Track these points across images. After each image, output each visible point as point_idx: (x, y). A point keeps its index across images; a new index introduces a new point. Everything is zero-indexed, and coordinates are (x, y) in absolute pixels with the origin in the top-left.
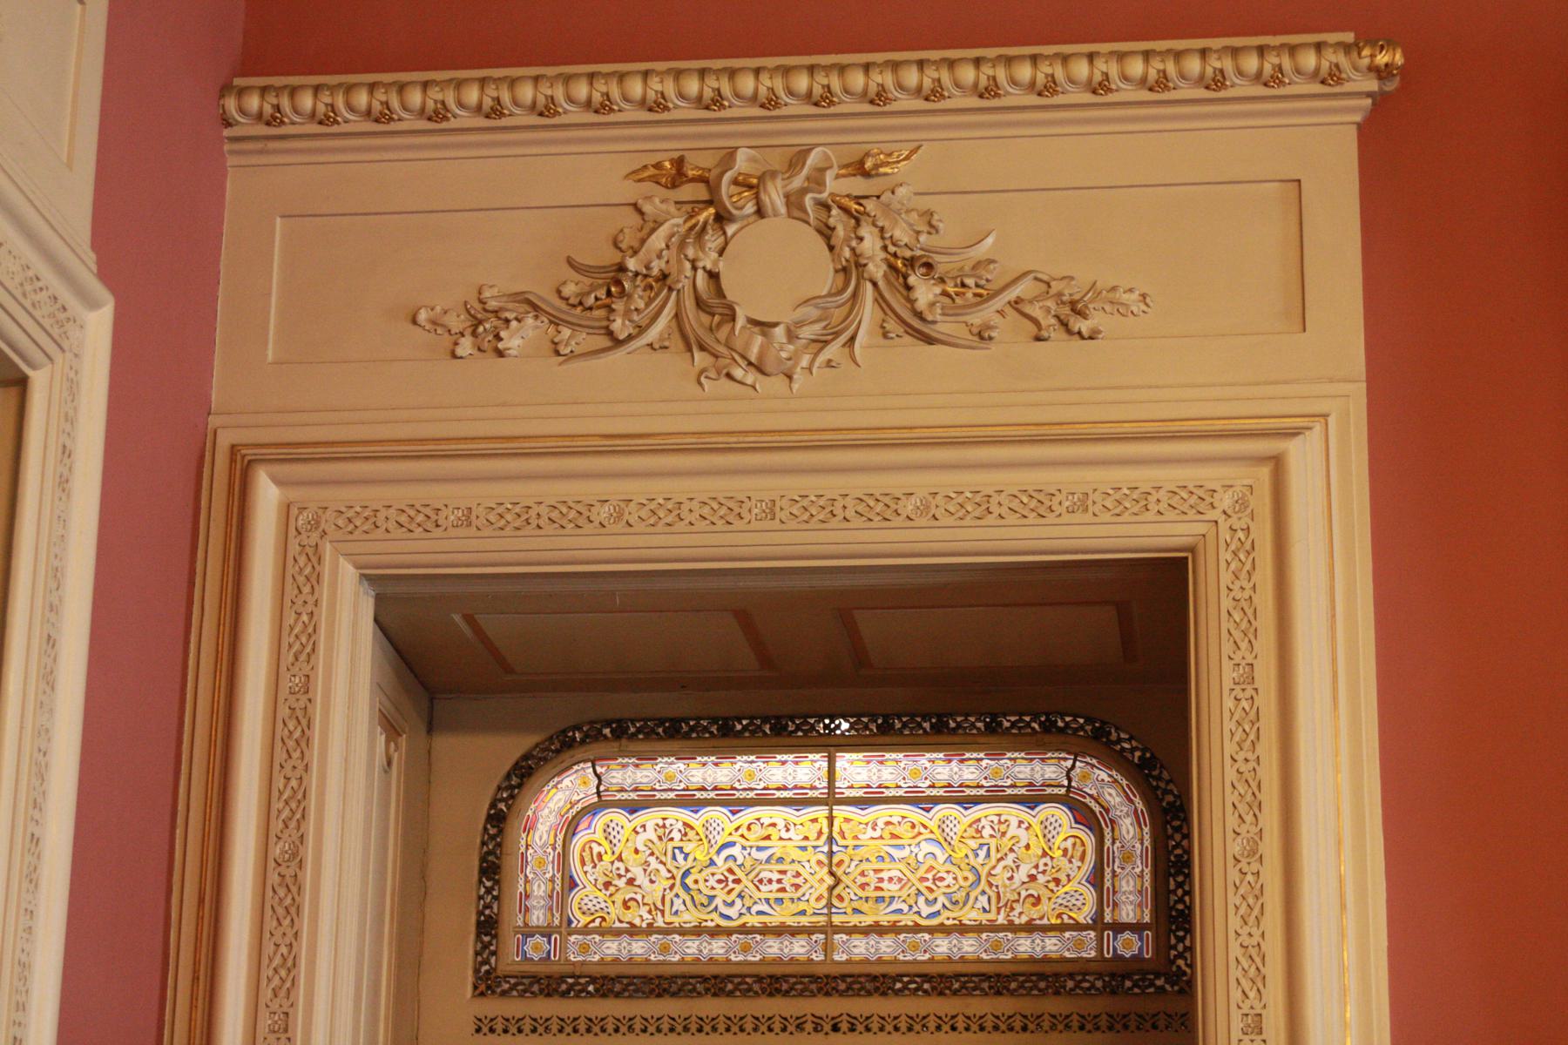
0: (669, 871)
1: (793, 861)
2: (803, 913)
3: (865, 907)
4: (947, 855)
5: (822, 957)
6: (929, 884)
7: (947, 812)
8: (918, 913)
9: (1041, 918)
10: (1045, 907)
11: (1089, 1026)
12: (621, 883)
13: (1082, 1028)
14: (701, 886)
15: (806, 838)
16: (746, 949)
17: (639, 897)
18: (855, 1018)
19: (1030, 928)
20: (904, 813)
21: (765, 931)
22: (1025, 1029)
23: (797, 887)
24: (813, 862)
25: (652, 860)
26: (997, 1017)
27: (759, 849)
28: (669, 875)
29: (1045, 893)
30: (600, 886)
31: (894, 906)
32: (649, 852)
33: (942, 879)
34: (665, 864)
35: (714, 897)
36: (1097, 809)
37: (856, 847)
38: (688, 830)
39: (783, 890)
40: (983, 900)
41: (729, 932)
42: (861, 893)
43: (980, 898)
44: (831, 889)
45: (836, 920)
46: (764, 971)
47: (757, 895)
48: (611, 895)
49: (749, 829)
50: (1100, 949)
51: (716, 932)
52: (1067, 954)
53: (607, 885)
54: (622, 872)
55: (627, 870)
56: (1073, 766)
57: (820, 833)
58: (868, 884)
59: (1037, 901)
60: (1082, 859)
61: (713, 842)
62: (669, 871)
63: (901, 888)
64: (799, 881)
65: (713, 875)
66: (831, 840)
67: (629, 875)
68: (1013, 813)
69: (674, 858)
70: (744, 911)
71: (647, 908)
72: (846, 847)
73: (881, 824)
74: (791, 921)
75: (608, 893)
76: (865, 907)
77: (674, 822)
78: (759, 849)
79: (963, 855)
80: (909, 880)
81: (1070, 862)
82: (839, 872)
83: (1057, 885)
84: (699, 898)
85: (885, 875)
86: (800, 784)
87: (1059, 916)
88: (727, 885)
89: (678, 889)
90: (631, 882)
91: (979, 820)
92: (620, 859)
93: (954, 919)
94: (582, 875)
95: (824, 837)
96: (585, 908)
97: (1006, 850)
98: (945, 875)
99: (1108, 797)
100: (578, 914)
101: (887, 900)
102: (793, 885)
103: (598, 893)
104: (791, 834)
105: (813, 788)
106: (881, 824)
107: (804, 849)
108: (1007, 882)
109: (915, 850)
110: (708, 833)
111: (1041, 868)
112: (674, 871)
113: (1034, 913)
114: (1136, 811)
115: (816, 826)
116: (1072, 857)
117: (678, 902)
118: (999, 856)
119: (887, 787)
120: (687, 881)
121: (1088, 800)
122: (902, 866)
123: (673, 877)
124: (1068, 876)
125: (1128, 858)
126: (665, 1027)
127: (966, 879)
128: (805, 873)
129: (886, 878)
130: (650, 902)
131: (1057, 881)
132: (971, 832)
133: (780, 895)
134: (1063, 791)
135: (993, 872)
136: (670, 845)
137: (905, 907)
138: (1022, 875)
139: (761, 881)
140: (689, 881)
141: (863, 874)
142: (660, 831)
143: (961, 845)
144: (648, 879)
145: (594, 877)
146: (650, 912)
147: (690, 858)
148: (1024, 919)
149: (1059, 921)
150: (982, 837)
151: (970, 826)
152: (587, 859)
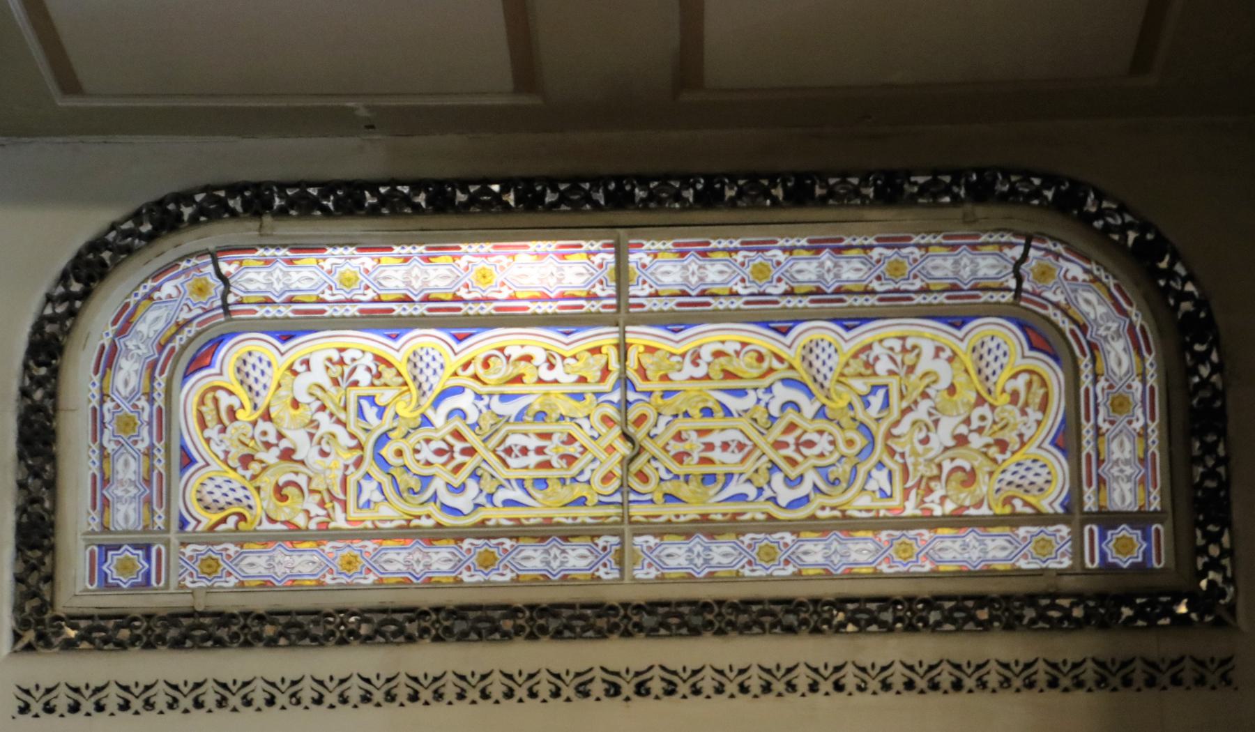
0: (353, 436)
1: (562, 417)
2: (581, 502)
3: (683, 491)
4: (817, 405)
5: (615, 574)
6: (790, 452)
7: (816, 335)
8: (773, 500)
9: (978, 505)
10: (984, 486)
11: (1065, 682)
12: (271, 456)
13: (1053, 683)
14: (408, 459)
15: (582, 380)
16: (487, 563)
17: (302, 480)
18: (674, 673)
19: (958, 521)
20: (745, 337)
21: (519, 532)
22: (957, 686)
23: (570, 459)
24: (596, 419)
25: (323, 417)
26: (911, 668)
27: (504, 397)
28: (353, 443)
29: (983, 466)
30: (234, 462)
31: (732, 489)
32: (317, 404)
33: (810, 444)
34: (344, 425)
35: (431, 477)
36: (1067, 326)
37: (666, 394)
38: (382, 367)
39: (547, 465)
40: (881, 477)
41: (458, 536)
42: (676, 468)
43: (875, 473)
44: (628, 461)
45: (638, 512)
46: (519, 597)
47: (502, 473)
48: (254, 477)
49: (486, 364)
50: (1078, 553)
51: (434, 535)
52: (1023, 564)
53: (246, 460)
54: (272, 438)
55: (281, 436)
56: (1025, 256)
57: (606, 371)
58: (688, 454)
59: (970, 477)
60: (1044, 407)
61: (426, 387)
62: (353, 436)
63: (743, 460)
64: (573, 450)
65: (428, 441)
66: (625, 382)
67: (284, 444)
68: (927, 334)
69: (361, 413)
70: (482, 499)
71: (317, 497)
72: (650, 393)
73: (706, 355)
74: (561, 515)
75: (248, 474)
76: (683, 491)
77: (358, 355)
78: (504, 397)
79: (843, 403)
80: (755, 446)
81: (1024, 413)
82: (640, 434)
83: (1003, 451)
84: (405, 480)
85: (716, 439)
86: (569, 291)
87: (1008, 501)
88: (452, 458)
89: (369, 465)
90: (287, 454)
91: (869, 347)
92: (267, 417)
93: (833, 508)
94: (202, 445)
95: (612, 378)
96: (208, 499)
97: (915, 395)
98: (815, 437)
99: (1085, 307)
100: (197, 510)
101: (721, 479)
102: (563, 457)
103: (232, 475)
104: (558, 373)
105: (592, 297)
106: (706, 355)
107: (579, 397)
108: (920, 448)
109: (766, 398)
110: (417, 372)
111: (975, 424)
112: (362, 436)
113: (966, 498)
114: (1132, 327)
115: (599, 360)
116: (1026, 404)
117: (369, 489)
118: (904, 404)
119: (714, 295)
120: (384, 452)
121: (1050, 312)
122: (744, 423)
123: (360, 446)
124: (1021, 436)
125: (1120, 404)
126: (354, 694)
127: (850, 443)
128: (582, 437)
129: (718, 443)
130: (322, 488)
131: (1002, 445)
132: (857, 366)
133: (542, 473)
134: (1009, 297)
135: (895, 431)
136: (353, 393)
137: (751, 491)
138: (943, 436)
139: (509, 451)
140: (388, 452)
141: (678, 437)
142: (335, 371)
143: (840, 388)
144: (316, 449)
145: (223, 447)
146: (322, 504)
147: (389, 414)
148: (950, 507)
149: (1007, 510)
150: (875, 374)
151: (855, 356)
152: (210, 418)
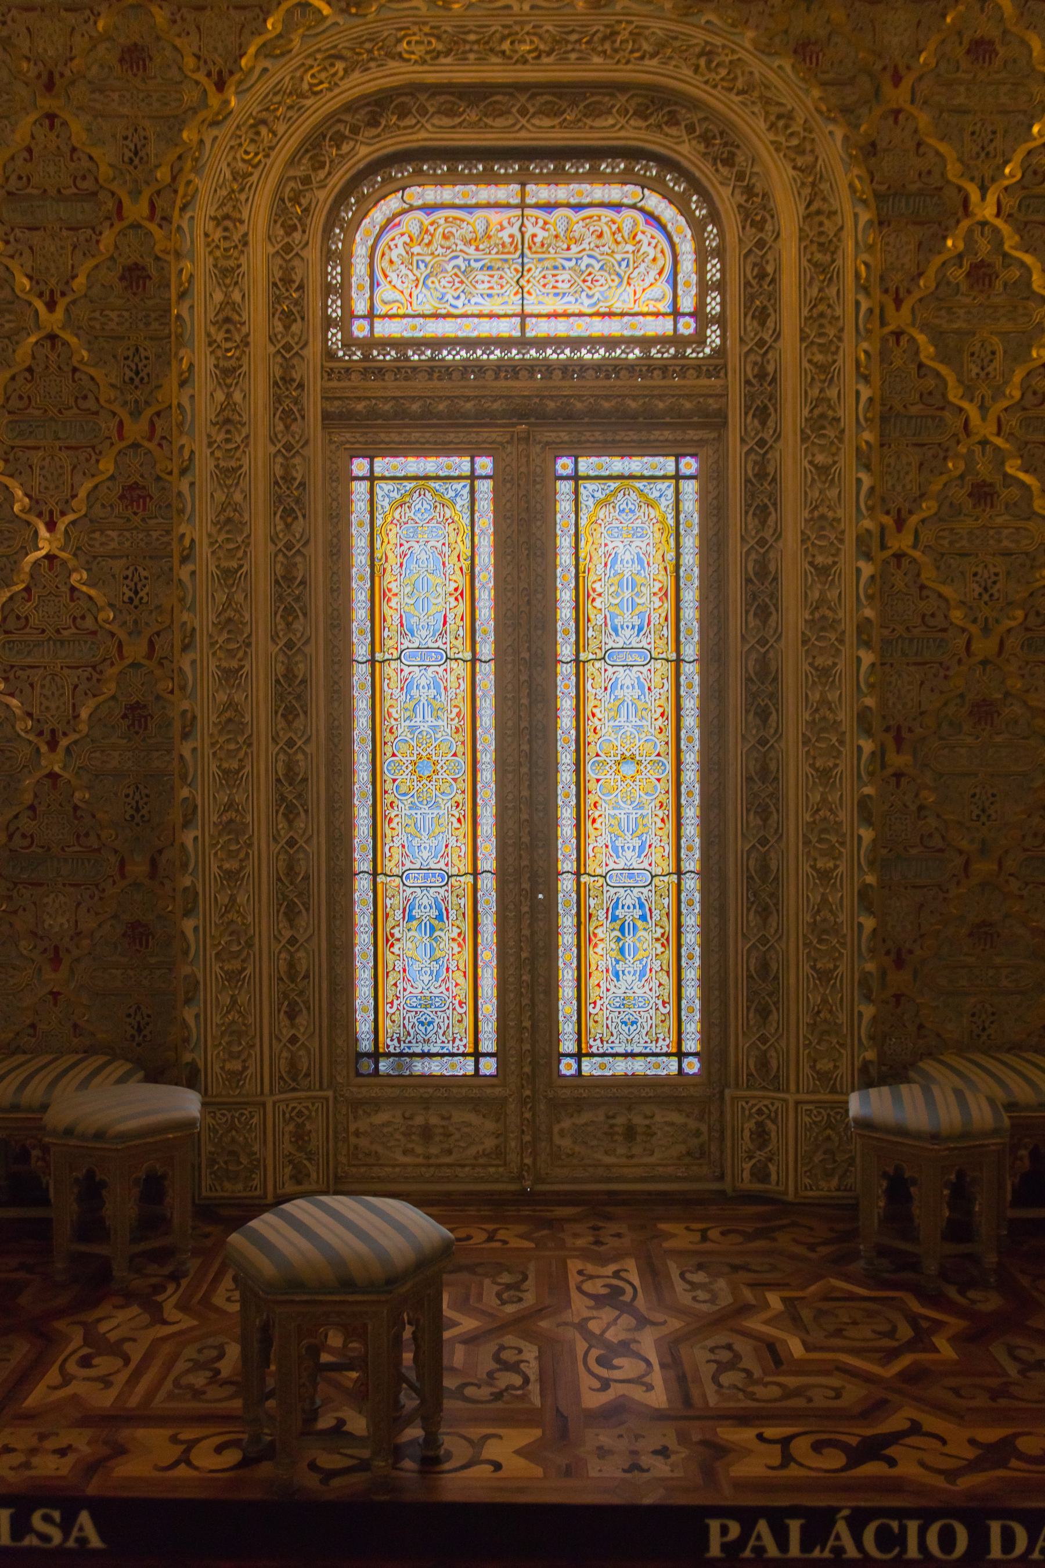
69: (418, 267)
